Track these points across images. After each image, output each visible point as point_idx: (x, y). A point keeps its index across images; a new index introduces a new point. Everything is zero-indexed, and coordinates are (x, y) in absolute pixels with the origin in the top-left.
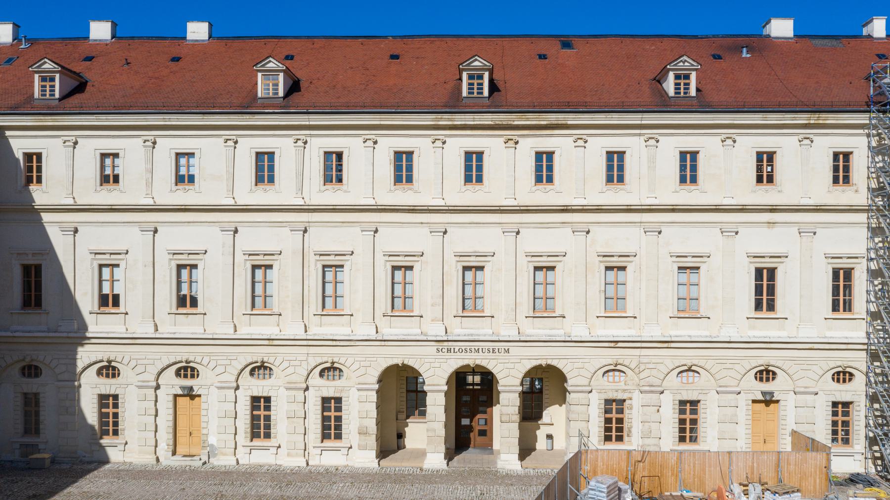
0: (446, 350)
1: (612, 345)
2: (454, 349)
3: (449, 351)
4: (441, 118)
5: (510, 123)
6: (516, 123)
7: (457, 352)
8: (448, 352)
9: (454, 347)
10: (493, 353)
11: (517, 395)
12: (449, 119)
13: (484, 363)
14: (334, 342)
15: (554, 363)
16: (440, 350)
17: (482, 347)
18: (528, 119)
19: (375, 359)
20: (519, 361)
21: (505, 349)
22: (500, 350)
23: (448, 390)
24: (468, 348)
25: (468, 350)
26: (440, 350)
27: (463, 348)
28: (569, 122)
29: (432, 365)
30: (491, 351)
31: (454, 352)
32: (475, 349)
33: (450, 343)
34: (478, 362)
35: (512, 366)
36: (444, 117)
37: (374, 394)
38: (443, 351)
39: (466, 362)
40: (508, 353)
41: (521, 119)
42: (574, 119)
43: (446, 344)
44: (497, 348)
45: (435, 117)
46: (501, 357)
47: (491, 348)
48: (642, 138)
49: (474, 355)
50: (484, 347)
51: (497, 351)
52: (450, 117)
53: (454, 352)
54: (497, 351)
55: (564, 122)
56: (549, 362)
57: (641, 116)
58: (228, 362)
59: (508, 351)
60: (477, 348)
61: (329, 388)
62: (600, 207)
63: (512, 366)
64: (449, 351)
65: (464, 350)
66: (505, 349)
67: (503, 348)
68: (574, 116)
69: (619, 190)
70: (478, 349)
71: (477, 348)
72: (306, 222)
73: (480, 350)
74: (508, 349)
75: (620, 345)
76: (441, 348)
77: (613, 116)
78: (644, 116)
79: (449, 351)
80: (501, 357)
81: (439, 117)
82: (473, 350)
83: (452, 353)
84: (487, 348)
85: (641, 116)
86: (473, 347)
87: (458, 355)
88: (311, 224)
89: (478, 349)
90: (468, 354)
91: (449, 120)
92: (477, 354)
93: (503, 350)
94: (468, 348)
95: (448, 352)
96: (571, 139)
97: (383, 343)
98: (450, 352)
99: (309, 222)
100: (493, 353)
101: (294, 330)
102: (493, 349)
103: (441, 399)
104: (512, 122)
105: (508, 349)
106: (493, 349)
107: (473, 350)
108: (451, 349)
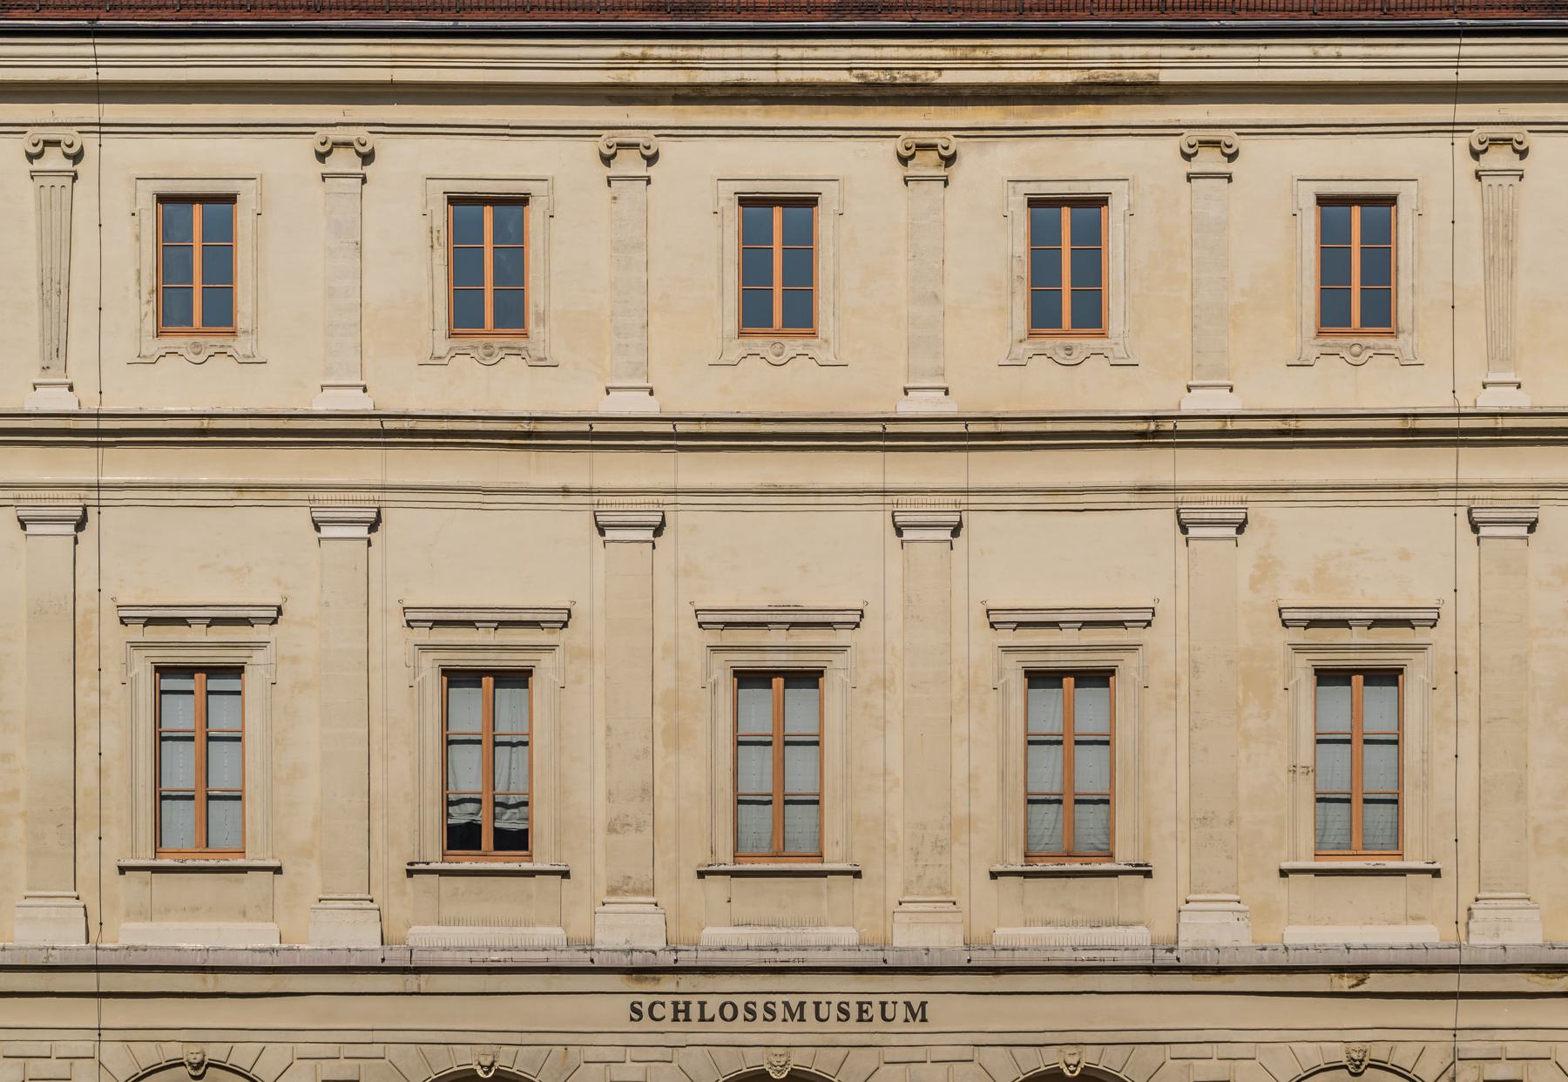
1: (1345, 983)
2: (702, 1004)
3: (681, 1016)
4: (644, 58)
5: (924, 77)
6: (948, 78)
7: (712, 1020)
8: (676, 1019)
9: (702, 998)
10: (860, 1020)
12: (673, 59)
16: (645, 1010)
17: (817, 998)
18: (996, 64)
19: (377, 1050)
20: (966, 1053)
21: (908, 1004)
22: (889, 1008)
24: (761, 1001)
25: (760, 1011)
26: (645, 1010)
27: (740, 1001)
28: (1165, 76)
30: (854, 1011)
31: (702, 1019)
32: (786, 1004)
33: (687, 982)
34: (799, 1059)
36: (655, 52)
38: (657, 1014)
40: (924, 1020)
41: (969, 63)
42: (1184, 63)
43: (668, 983)
44: (876, 1000)
45: (616, 52)
46: (894, 1040)
47: (853, 1000)
48: (1462, 141)
49: (782, 1031)
50: (823, 999)
51: (875, 1011)
52: (680, 53)
53: (702, 1019)
54: (875, 1011)
55: (1142, 75)
56: (1090, 1057)
57: (1454, 51)
59: (918, 1013)
60: (794, 1001)
62: (1292, 424)
64: (681, 1016)
65: (741, 1012)
66: (908, 1004)
67: (901, 999)
68: (1186, 52)
69: (1370, 353)
70: (801, 1004)
71: (794, 1001)
72: (89, 487)
73: (809, 1010)
74: (923, 1004)
75: (1375, 982)
76: (646, 1001)
77: (1345, 51)
78: (1465, 51)
79: (681, 1013)
80: (894, 1040)
81: (637, 52)
82: (780, 1010)
83: (695, 1025)
84: (836, 999)
85: (1454, 51)
86: (779, 999)
87: (720, 1031)
88: (104, 494)
89: (801, 1004)
90: (760, 1024)
91: (675, 64)
92: (794, 1025)
93: (901, 1009)
94: (761, 1001)
95: (676, 1019)
96: (1169, 148)
97: (412, 983)
98: (687, 1019)
99: (99, 487)
100: (860, 1020)
102: (860, 1004)
104: (932, 74)
105: (923, 1004)
106: (860, 1004)
108: (687, 1004)
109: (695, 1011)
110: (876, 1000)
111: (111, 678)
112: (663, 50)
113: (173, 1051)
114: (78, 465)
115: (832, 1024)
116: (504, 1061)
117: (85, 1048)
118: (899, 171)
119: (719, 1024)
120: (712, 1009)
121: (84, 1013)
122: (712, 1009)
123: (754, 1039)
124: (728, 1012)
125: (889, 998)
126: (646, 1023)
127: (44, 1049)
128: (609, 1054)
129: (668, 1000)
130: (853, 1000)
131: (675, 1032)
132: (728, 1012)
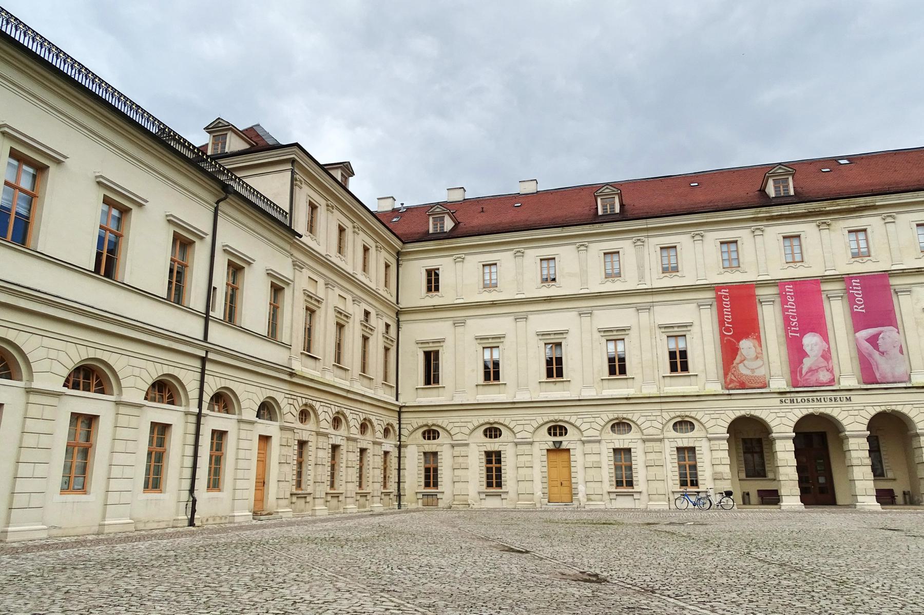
0: (789, 401)
4: (760, 212)
6: (828, 209)
11: (866, 440)
13: (828, 411)
14: (684, 398)
15: (899, 408)
18: (838, 205)
20: (862, 408)
21: (846, 398)
23: (796, 436)
24: (811, 398)
25: (811, 400)
27: (806, 398)
28: (877, 204)
29: (779, 415)
30: (833, 399)
32: (817, 399)
33: (792, 395)
34: (822, 410)
35: (856, 413)
37: (725, 442)
39: (811, 411)
43: (788, 395)
44: (838, 397)
46: (844, 406)
47: (833, 397)
51: (838, 399)
53: (797, 402)
54: (838, 399)
55: (872, 204)
56: (894, 408)
58: (592, 420)
61: (685, 439)
62: (920, 270)
63: (856, 413)
66: (846, 398)
67: (844, 397)
70: (820, 399)
72: (651, 302)
73: (822, 400)
74: (850, 398)
76: (784, 399)
80: (844, 406)
82: (815, 400)
83: (795, 404)
86: (815, 398)
87: (802, 405)
89: (820, 399)
90: (811, 403)
91: (767, 212)
92: (819, 403)
93: (845, 399)
94: (811, 398)
97: (729, 397)
99: (653, 302)
101: (650, 390)
103: (791, 446)
105: (850, 398)
107: (815, 400)
109: (795, 401)
110: (838, 397)
111: (658, 339)
112: (764, 209)
113: (678, 414)
114: (649, 299)
115: (828, 403)
116: (753, 413)
117: (659, 414)
118: (817, 229)
119: (801, 404)
120: (799, 400)
121: (658, 407)
122: (799, 400)
123: (810, 407)
124: (803, 401)
125: (842, 397)
126: (784, 404)
127: (650, 414)
128: (776, 411)
129: (789, 399)
130: (833, 397)
131: (792, 406)
132: (803, 401)
